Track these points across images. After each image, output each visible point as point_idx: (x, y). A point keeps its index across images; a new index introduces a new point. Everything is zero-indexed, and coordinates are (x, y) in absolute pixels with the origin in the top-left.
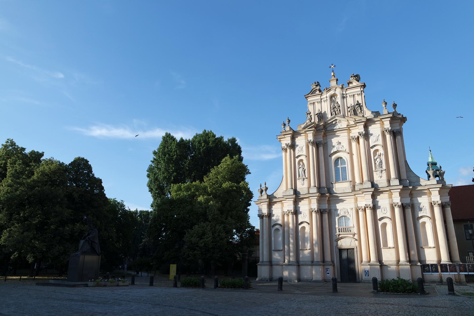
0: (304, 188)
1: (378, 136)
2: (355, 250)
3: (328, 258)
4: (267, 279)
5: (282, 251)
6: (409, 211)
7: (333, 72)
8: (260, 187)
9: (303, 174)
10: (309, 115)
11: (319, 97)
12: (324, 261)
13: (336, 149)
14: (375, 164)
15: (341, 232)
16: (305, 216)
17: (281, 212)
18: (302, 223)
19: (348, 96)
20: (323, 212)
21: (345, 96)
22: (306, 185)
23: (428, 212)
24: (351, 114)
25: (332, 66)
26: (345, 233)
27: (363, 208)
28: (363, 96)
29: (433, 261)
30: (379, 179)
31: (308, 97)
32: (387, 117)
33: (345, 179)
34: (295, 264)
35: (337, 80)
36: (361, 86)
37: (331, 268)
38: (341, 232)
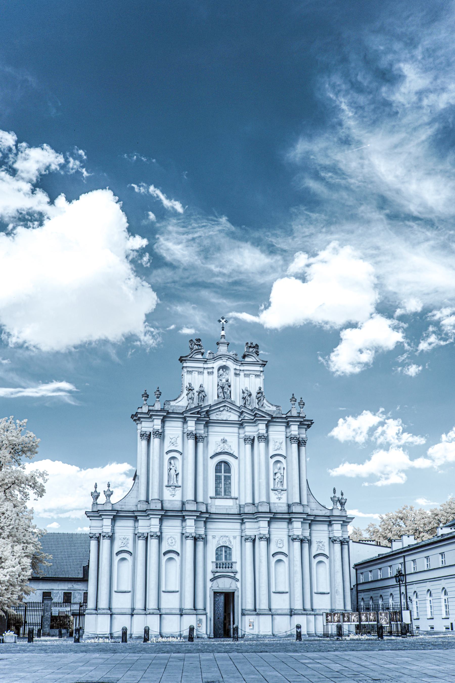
0: (176, 501)
1: (281, 442)
2: (236, 594)
3: (200, 605)
4: (106, 636)
5: (129, 593)
6: (306, 546)
7: (223, 330)
8: (94, 489)
9: (175, 479)
10: (191, 392)
11: (201, 365)
12: (195, 609)
13: (220, 448)
14: (275, 479)
15: (218, 568)
16: (174, 543)
19: (242, 374)
20: (198, 538)
21: (238, 372)
22: (178, 497)
24: (247, 403)
25: (223, 321)
26: (224, 570)
27: (253, 537)
28: (262, 378)
29: (327, 609)
30: (277, 501)
31: (185, 360)
32: (297, 420)
35: (228, 345)
36: (262, 364)
37: (203, 618)
38: (218, 568)
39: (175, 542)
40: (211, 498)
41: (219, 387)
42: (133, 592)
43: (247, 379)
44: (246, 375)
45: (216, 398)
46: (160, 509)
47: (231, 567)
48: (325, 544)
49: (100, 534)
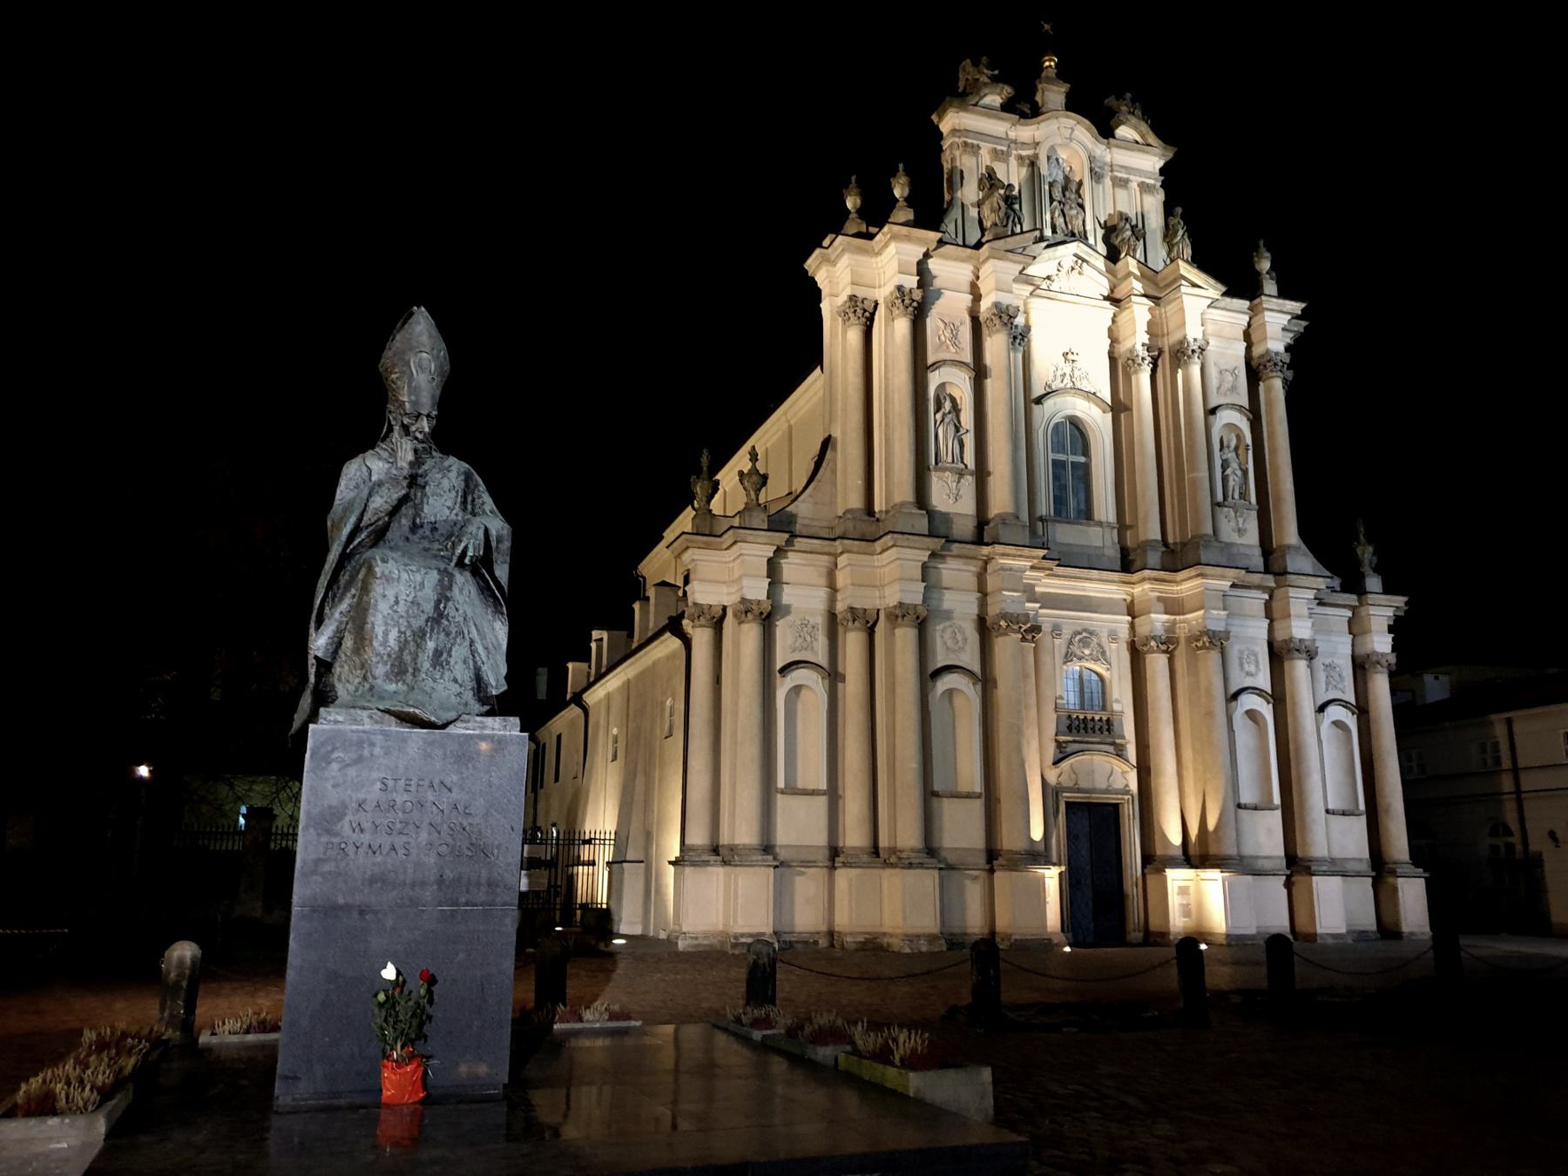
16: (960, 643)
17: (827, 608)
18: (949, 669)
23: (1347, 690)
29: (1360, 860)
33: (1087, 514)
34: (1365, 867)
39: (965, 640)
40: (1041, 519)
41: (1055, 203)
42: (833, 794)
43: (1121, 194)
44: (1121, 183)
45: (1048, 232)
46: (927, 533)
47: (1108, 730)
48: (1344, 674)
49: (724, 609)
